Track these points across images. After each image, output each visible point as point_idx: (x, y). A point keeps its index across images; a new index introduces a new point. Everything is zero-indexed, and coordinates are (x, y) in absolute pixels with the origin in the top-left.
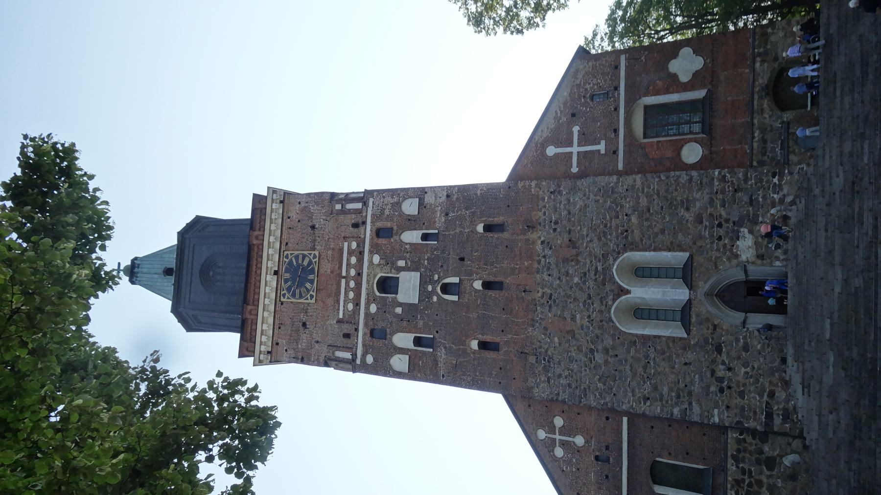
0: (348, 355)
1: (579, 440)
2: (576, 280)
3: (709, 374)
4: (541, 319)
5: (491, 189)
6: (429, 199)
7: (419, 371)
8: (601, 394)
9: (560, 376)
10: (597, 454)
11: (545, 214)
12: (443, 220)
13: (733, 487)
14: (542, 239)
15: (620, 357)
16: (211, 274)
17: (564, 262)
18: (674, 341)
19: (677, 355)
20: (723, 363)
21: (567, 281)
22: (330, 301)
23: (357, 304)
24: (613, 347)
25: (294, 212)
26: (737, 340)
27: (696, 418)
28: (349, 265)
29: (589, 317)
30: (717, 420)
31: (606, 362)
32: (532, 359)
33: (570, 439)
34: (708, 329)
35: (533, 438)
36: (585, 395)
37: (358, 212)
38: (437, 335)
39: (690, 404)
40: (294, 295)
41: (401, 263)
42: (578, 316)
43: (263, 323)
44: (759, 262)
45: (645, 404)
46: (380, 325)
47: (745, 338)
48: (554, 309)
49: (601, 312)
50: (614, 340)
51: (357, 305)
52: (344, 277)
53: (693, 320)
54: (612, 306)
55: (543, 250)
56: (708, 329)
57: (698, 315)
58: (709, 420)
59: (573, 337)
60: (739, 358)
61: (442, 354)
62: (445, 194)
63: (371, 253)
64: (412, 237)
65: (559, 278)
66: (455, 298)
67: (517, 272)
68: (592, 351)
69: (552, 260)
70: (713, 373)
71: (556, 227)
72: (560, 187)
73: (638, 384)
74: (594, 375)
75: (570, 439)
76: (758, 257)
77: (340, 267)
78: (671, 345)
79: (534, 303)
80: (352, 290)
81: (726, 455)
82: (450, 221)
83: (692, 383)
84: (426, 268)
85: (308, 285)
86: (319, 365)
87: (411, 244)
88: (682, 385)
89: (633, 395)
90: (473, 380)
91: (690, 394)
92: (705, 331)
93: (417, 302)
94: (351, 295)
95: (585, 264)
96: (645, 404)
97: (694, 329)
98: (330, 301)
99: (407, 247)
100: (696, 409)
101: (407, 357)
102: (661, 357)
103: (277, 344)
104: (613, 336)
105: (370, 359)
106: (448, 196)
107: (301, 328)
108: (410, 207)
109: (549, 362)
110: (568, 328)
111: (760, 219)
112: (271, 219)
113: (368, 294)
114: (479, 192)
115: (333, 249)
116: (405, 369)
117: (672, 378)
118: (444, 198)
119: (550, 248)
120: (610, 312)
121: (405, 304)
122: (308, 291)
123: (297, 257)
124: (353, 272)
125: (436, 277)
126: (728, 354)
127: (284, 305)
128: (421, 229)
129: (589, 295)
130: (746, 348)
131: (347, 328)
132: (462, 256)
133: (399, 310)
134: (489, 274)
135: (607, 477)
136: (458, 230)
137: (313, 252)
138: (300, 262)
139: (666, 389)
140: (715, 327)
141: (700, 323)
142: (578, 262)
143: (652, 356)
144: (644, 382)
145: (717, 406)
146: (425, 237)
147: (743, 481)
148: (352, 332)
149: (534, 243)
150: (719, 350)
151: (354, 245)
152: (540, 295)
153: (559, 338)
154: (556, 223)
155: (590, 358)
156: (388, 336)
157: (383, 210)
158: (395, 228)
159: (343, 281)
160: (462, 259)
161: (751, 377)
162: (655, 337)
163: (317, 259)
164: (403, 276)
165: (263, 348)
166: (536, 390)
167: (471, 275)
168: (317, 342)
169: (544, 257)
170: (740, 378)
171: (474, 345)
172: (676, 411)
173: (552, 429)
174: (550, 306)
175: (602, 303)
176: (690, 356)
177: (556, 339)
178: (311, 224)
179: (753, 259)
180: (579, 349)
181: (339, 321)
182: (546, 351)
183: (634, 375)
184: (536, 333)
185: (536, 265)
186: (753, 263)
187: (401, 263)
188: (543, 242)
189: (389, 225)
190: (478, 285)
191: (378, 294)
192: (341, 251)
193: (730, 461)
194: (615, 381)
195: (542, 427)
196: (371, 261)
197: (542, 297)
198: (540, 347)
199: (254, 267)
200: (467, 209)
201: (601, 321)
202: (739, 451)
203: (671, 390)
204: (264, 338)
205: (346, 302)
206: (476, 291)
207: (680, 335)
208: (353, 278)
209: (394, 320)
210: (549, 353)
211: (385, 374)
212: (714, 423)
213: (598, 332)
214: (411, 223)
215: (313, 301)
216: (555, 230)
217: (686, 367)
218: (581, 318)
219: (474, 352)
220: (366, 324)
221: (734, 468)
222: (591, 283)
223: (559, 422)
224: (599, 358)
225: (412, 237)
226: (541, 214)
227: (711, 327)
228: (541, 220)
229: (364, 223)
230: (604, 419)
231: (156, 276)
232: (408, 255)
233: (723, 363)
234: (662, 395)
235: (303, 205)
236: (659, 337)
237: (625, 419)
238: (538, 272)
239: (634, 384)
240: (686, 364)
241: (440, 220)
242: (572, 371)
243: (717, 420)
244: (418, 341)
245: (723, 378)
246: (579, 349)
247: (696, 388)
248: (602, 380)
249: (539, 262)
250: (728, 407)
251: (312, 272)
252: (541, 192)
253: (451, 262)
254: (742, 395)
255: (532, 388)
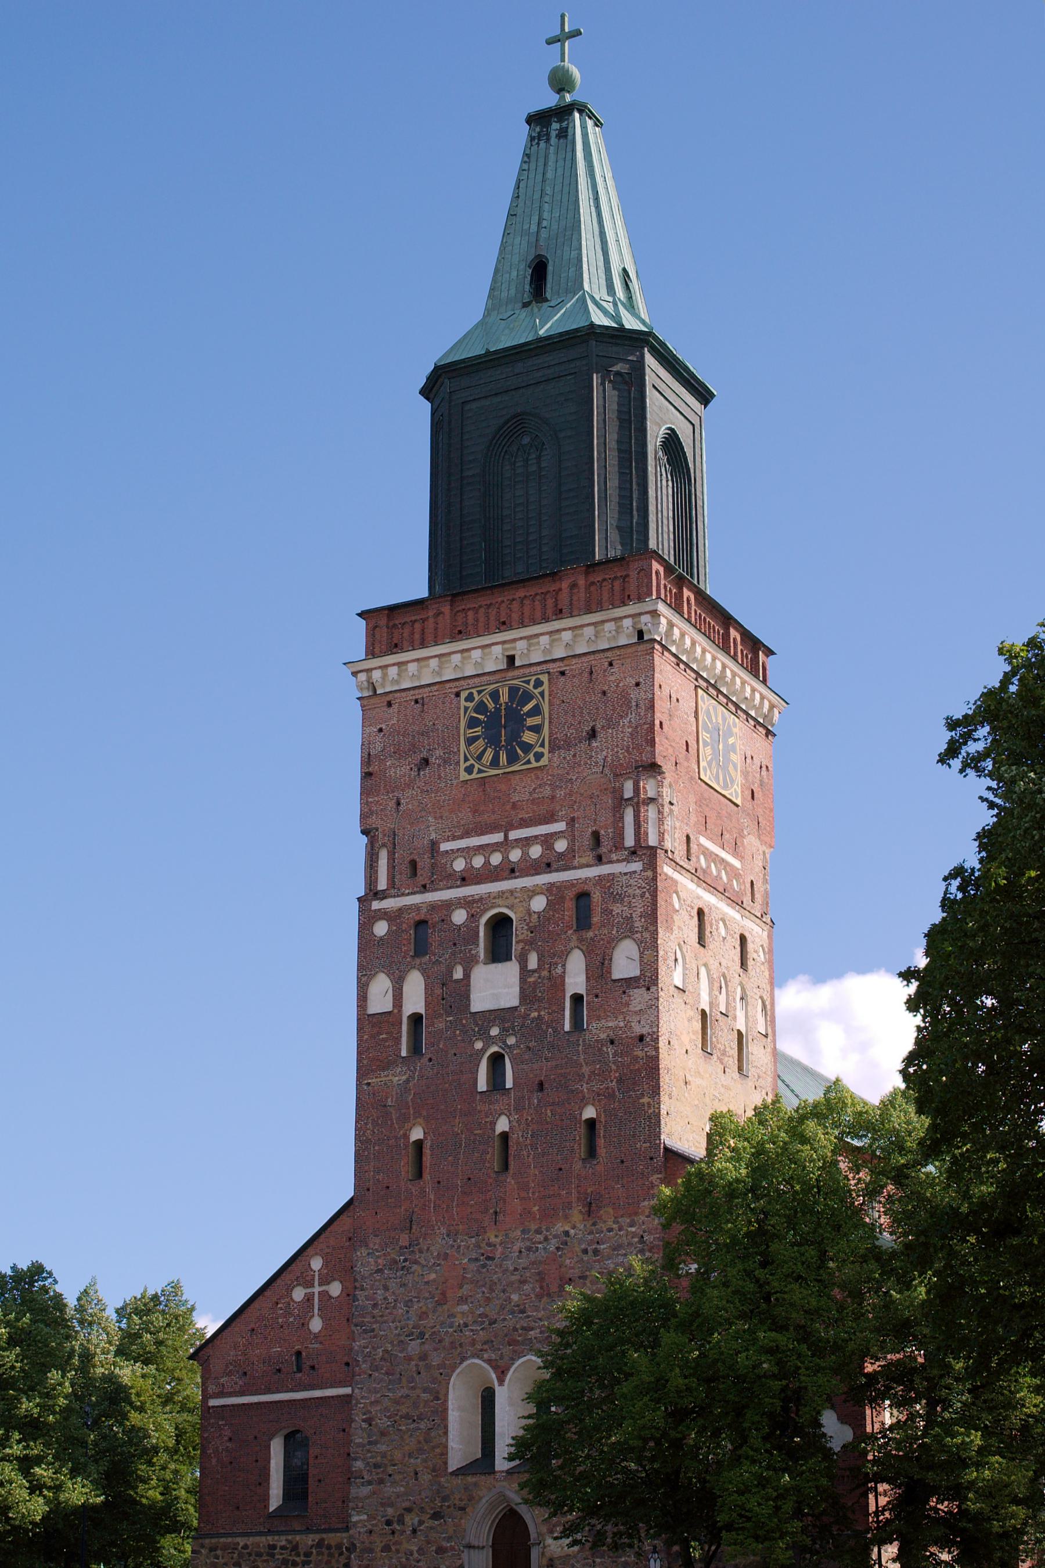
0: (382, 884)
1: (316, 1325)
2: (515, 1297)
3: (407, 1504)
4: (459, 1247)
5: (654, 1122)
6: (638, 997)
7: (372, 1036)
8: (369, 1355)
9: (386, 1288)
10: (304, 1354)
11: (610, 1230)
12: (603, 1036)
13: (289, 1542)
14: (572, 1232)
15: (417, 1378)
16: (526, 440)
17: (539, 1274)
18: (442, 1454)
19: (425, 1461)
20: (421, 1523)
21: (512, 1283)
22: (465, 816)
23: (464, 880)
24: (428, 1367)
25: (620, 677)
26: (449, 1539)
27: (354, 1491)
28: (527, 842)
29: (466, 1325)
30: (355, 1519)
31: (409, 1359)
32: (404, 1239)
33: (316, 1311)
34: (461, 1500)
35: (310, 1251)
36: (365, 1331)
37: (618, 844)
38: (425, 1060)
39: (370, 1483)
40: (472, 723)
41: (533, 962)
42: (465, 1307)
43: (418, 660)
44: (545, 1562)
45: (364, 1421)
46: (434, 938)
47: (452, 1548)
48: (473, 1266)
49: (473, 1343)
50: (439, 1366)
51: (463, 879)
52: (506, 836)
53: (470, 1479)
54: (481, 1359)
55: (555, 1237)
56: (461, 1500)
57: (476, 1484)
58: (353, 1509)
59: (439, 1303)
60: (428, 1543)
61: (397, 1077)
62: (644, 1031)
63: (549, 889)
64: (576, 977)
65: (516, 1269)
66: (482, 1085)
67: (523, 1194)
68: (422, 1335)
69: (541, 1254)
70: (409, 1510)
71: (590, 1253)
72: (650, 1251)
73: (387, 1409)
74: (391, 1343)
75: (316, 1311)
76: (551, 1560)
77: (524, 824)
78: (438, 1450)
79: (481, 1231)
80: (487, 862)
81: (325, 1531)
82: (600, 1050)
83: (394, 1483)
84: (526, 1016)
85: (489, 755)
86: (364, 816)
87: (562, 977)
88: (390, 1470)
89: (372, 1403)
90: (368, 1141)
91: (381, 1481)
92: (457, 1497)
93: (473, 1009)
94: (478, 862)
95: (537, 1309)
96: (364, 1421)
97: (458, 1481)
98: (465, 816)
99: (559, 970)
100: (366, 1490)
101: (388, 1007)
102: (421, 1439)
103: (389, 704)
104: (442, 1366)
105: (381, 928)
106: (641, 1038)
107: (417, 758)
108: (625, 962)
109: (403, 1268)
110: (449, 1294)
111: (598, 1560)
112: (603, 622)
113: (481, 899)
114: (645, 1100)
115: (553, 797)
116: (371, 1010)
117: (398, 1455)
118: (638, 1030)
119: (558, 1249)
120: (473, 1356)
121: (469, 985)
122: (479, 758)
123: (536, 711)
124: (515, 855)
125: (511, 1041)
126: (431, 1528)
127: (455, 701)
128: (587, 995)
129: (494, 1323)
130: (441, 1550)
131: (424, 862)
132: (546, 1086)
133: (458, 974)
134: (518, 1143)
135: (279, 1371)
136: (586, 1070)
137: (546, 751)
138: (530, 722)
139: (383, 1448)
140: (463, 1509)
141: (466, 1489)
142: (540, 1297)
143: (422, 1425)
144: (389, 1417)
145: (371, 1517)
146: (577, 999)
147: (298, 1555)
148: (421, 879)
149: (566, 1217)
150: (436, 1516)
151: (561, 846)
152: (493, 1239)
153: (434, 1280)
154: (596, 1252)
155: (412, 1334)
156: (418, 961)
157: (619, 898)
158: (590, 934)
159: (497, 837)
160: (541, 1086)
161: (407, 1559)
162: (446, 1427)
163: (535, 764)
164: (510, 970)
165: (377, 675)
166: (364, 1251)
167: (519, 1109)
168: (398, 804)
169: (546, 1239)
170: (406, 1546)
171: (417, 1134)
172: (359, 1464)
173: (325, 1281)
174: (477, 1260)
175: (485, 1343)
176: (425, 1478)
177: (433, 1276)
178: (598, 727)
179: (548, 1555)
180: (423, 1315)
181: (434, 845)
182: (416, 1262)
183: (397, 1402)
184: (439, 1243)
185: (533, 1227)
186: (543, 1554)
187: (533, 962)
188: (567, 1233)
189: (595, 919)
190: (502, 1125)
191: (484, 920)
192: (550, 818)
193: (317, 1537)
194: (387, 1373)
195: (325, 1265)
196: (532, 892)
197: (489, 1245)
198: (421, 1251)
199: (522, 595)
200: (620, 1081)
201: (461, 1345)
202: (329, 1547)
203: (384, 1455)
204: (393, 671)
205: (468, 853)
206: (493, 1124)
207: (450, 1462)
208: (506, 858)
209: (443, 968)
210: (415, 1267)
211: (361, 967)
212: (350, 1516)
213: (447, 1341)
214: (599, 969)
215: (464, 776)
216: (585, 1252)
217: (412, 1474)
218: (463, 1313)
219: (406, 1136)
220: (433, 907)
221: (310, 1543)
222: (511, 1321)
223: (335, 1289)
224: (414, 1347)
225: (576, 977)
226: (610, 1223)
227: (462, 1504)
228: (601, 1225)
229: (599, 860)
230: (346, 1359)
231: (534, 228)
232: (545, 973)
233: (421, 1523)
234: (376, 1443)
235: (634, 694)
236: (446, 1433)
237: (347, 1390)
238: (523, 1232)
239: (386, 1403)
240: (417, 1474)
241: (598, 1029)
242: (394, 1307)
243: (355, 1519)
244: (416, 1019)
245: (403, 1524)
246: (423, 1315)
247: (389, 1490)
248: (386, 1356)
249: (538, 1232)
250: (371, 1532)
251: (513, 759)
252: (642, 1218)
253: (535, 1066)
254: (386, 1548)
255: (367, 1246)
